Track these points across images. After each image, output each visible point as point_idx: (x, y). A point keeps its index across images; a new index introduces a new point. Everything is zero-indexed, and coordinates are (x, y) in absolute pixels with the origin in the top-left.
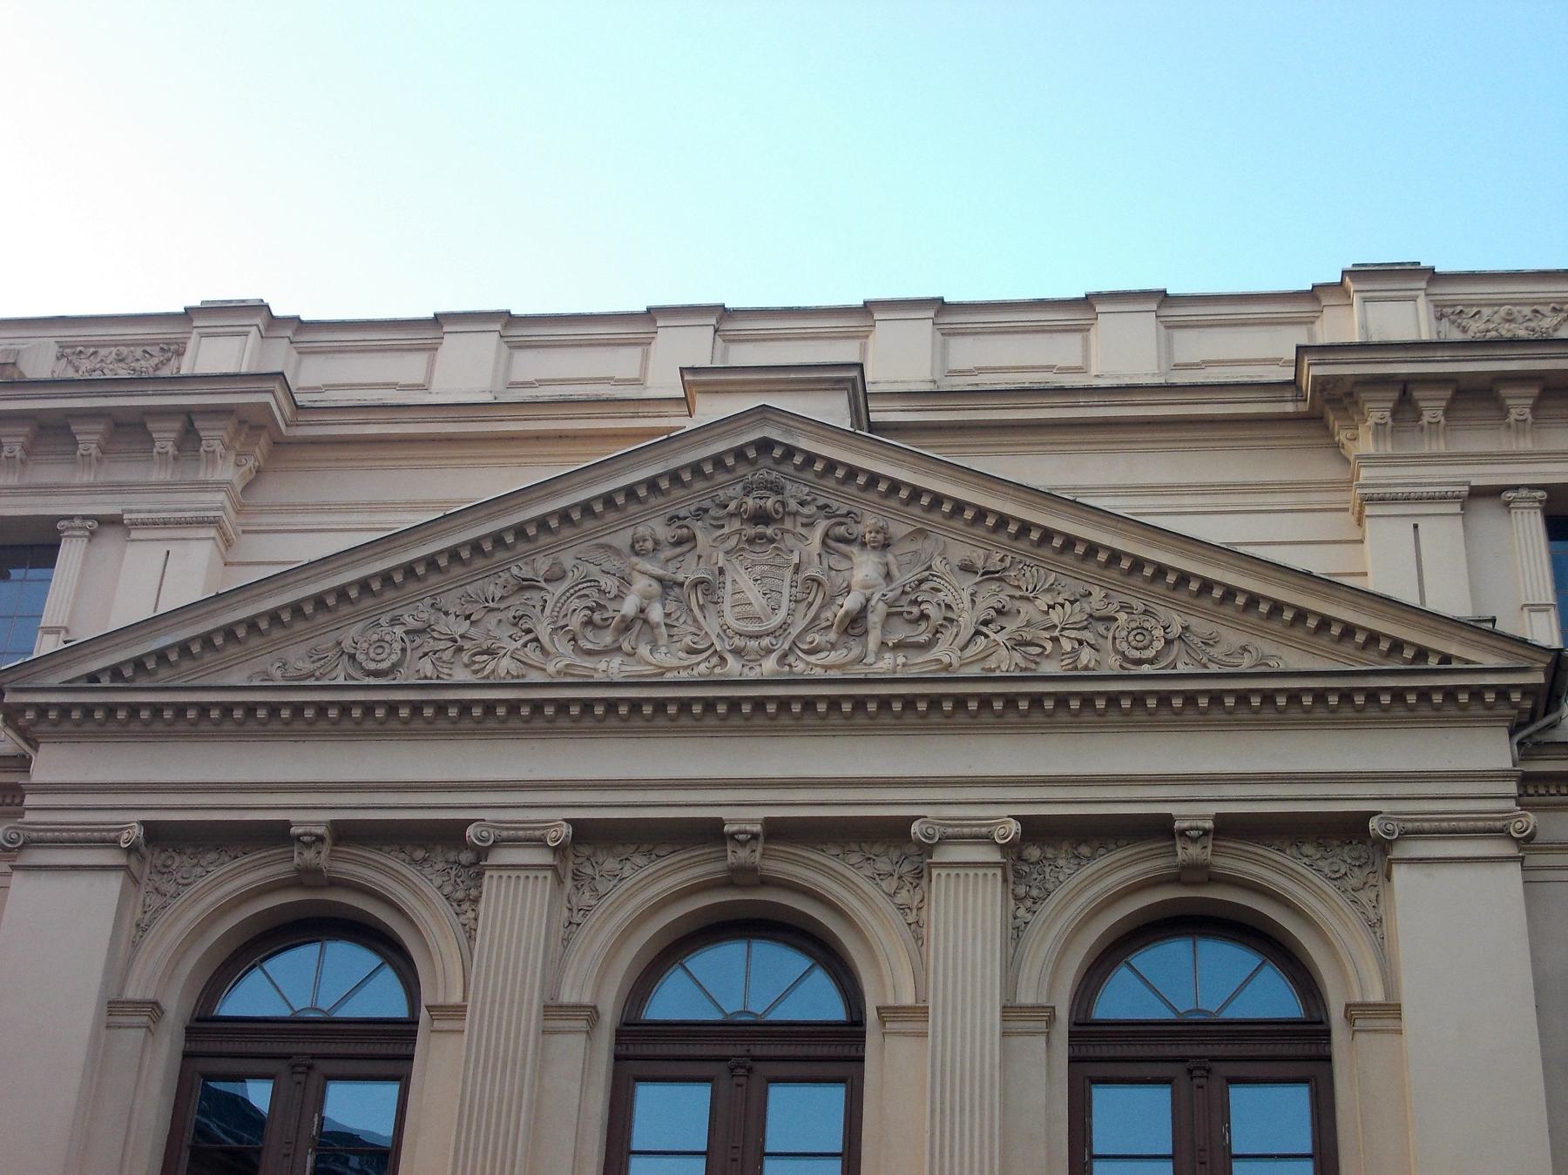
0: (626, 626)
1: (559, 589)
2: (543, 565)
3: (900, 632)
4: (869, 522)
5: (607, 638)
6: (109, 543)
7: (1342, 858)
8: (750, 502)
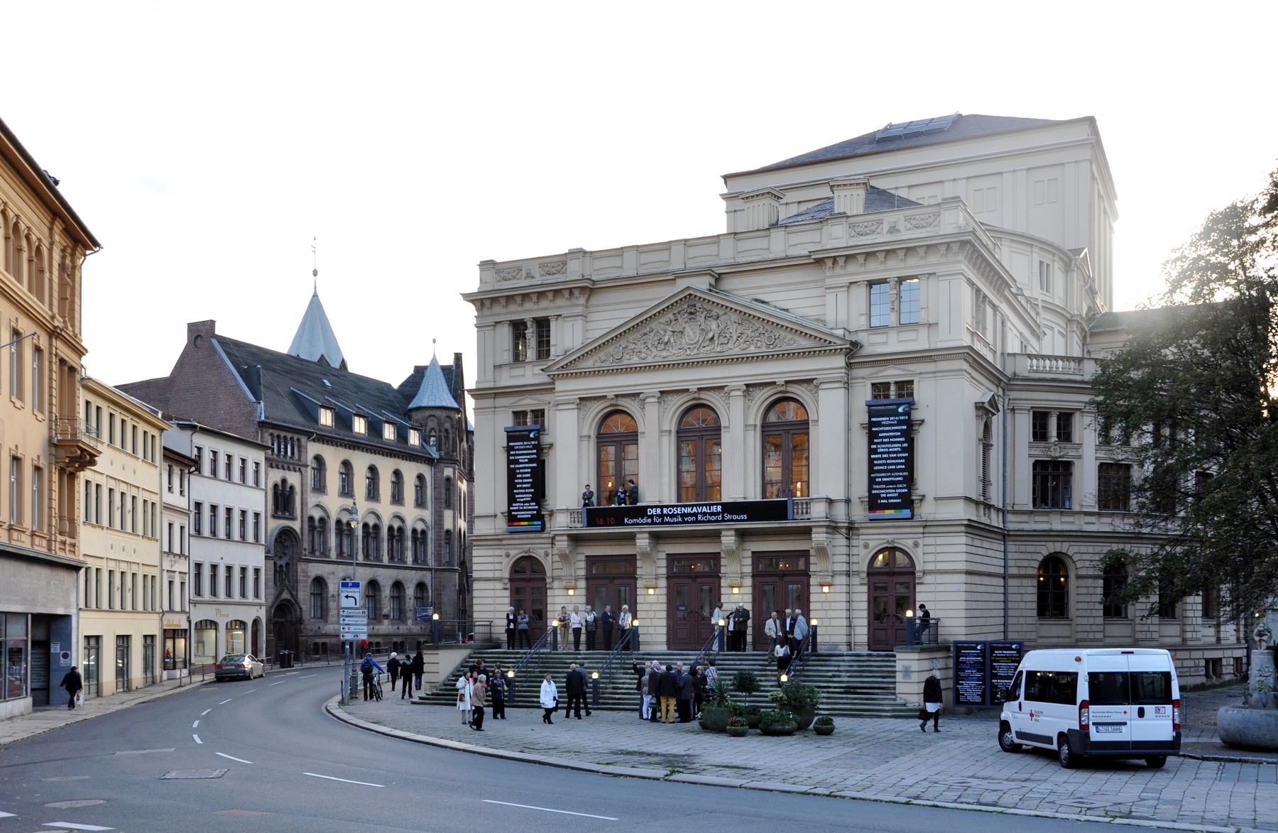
4: (714, 314)
7: (811, 387)
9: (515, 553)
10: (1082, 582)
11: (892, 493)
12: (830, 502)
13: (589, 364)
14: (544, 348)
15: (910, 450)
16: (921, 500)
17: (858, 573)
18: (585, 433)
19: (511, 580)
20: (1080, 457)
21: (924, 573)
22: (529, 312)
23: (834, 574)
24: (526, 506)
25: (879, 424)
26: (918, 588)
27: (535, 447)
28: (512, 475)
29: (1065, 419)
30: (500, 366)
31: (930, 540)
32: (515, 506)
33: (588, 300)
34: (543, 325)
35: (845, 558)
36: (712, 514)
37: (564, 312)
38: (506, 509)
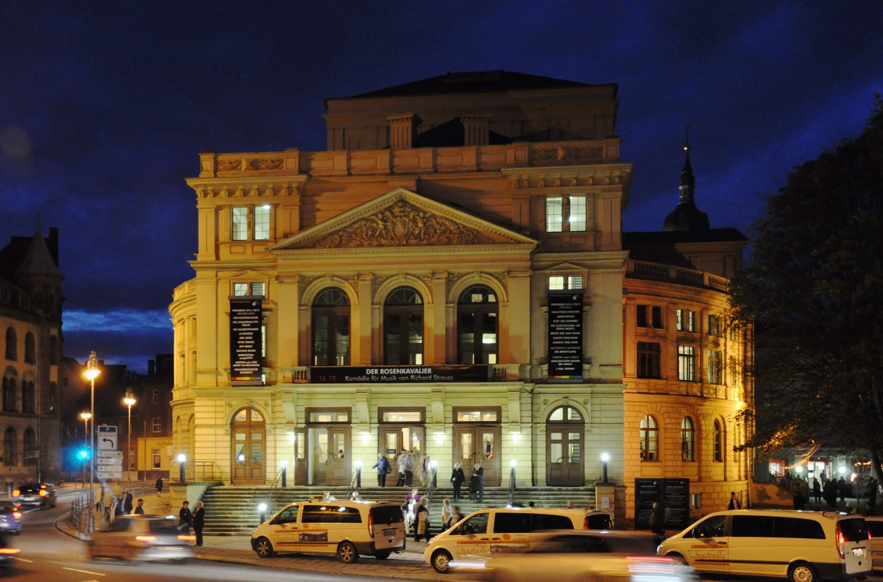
9: (237, 403)
11: (568, 363)
15: (580, 329)
24: (248, 364)
25: (557, 308)
27: (256, 314)
28: (234, 338)
32: (238, 364)
36: (422, 375)
38: (229, 366)
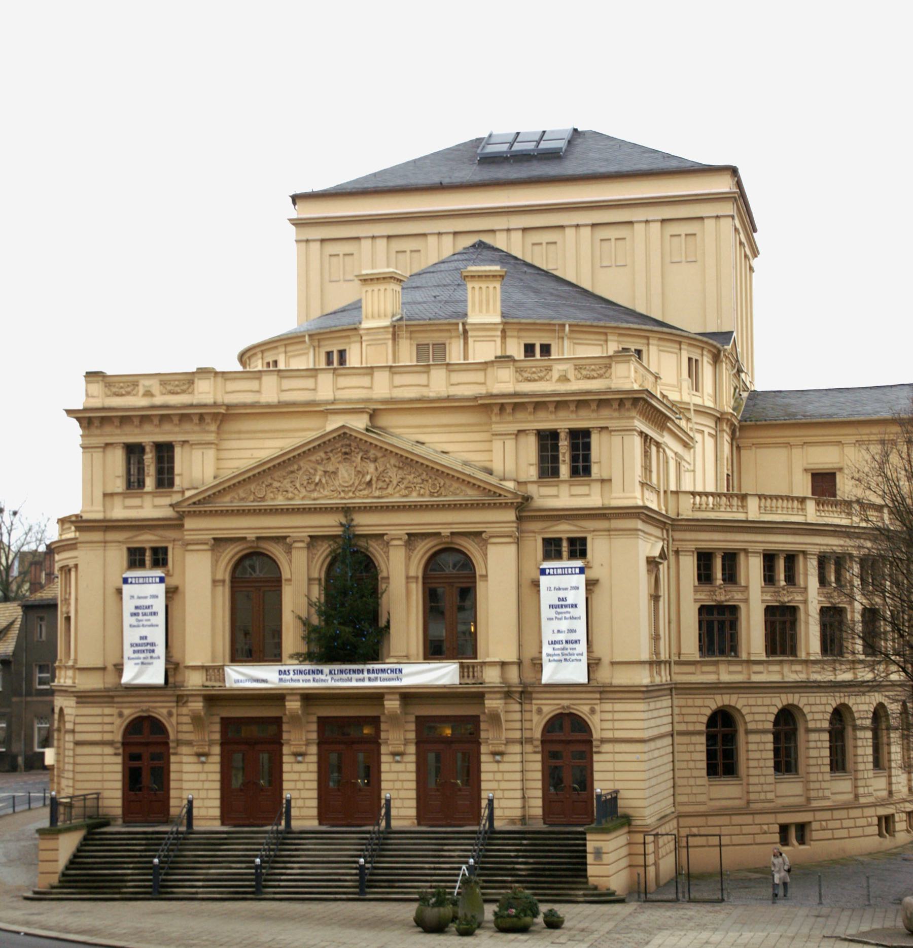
0: (317, 484)
1: (301, 472)
2: (296, 467)
3: (381, 484)
5: (312, 487)
6: (187, 447)
8: (343, 450)
9: (130, 712)
10: (753, 738)
12: (503, 664)
13: (226, 502)
14: (165, 479)
16: (597, 664)
17: (530, 741)
18: (219, 576)
19: (124, 744)
20: (746, 601)
21: (603, 741)
22: (148, 436)
23: (509, 742)
26: (596, 757)
29: (731, 559)
30: (112, 495)
31: (608, 707)
33: (219, 428)
34: (165, 452)
35: (518, 725)
37: (192, 438)
